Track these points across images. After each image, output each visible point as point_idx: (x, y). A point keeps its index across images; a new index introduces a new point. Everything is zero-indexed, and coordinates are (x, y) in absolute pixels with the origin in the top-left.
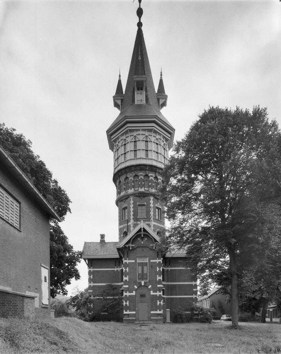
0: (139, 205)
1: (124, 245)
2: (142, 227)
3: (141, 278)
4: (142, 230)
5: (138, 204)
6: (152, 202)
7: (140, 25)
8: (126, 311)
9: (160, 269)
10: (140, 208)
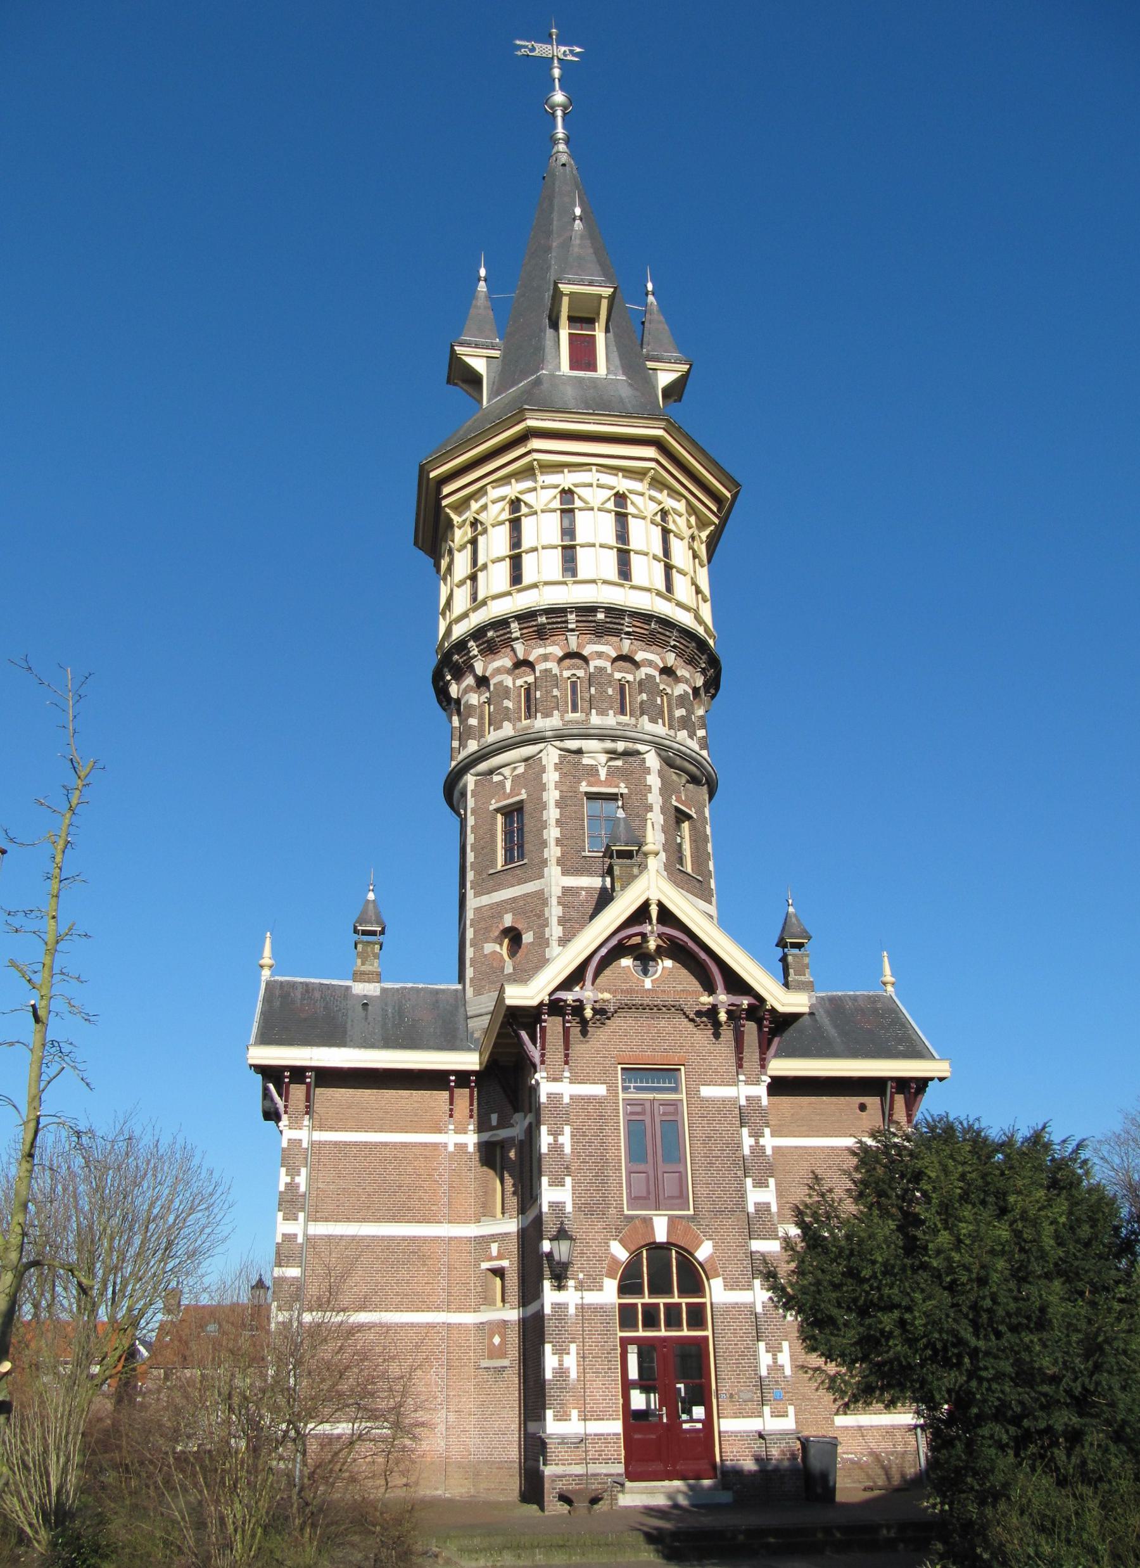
0: (591, 797)
1: (550, 995)
2: (654, 897)
3: (644, 1194)
4: (654, 911)
5: (584, 787)
8: (562, 1417)
9: (757, 1142)
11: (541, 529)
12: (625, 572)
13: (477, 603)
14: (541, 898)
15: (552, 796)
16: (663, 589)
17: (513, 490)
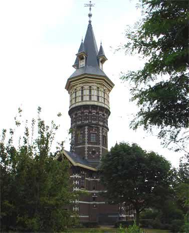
6: (86, 130)
7: (90, 22)
10: (92, 135)
11: (86, 92)
12: (98, 100)
13: (76, 103)
14: (84, 148)
15: (86, 133)
16: (103, 101)
17: (82, 85)
